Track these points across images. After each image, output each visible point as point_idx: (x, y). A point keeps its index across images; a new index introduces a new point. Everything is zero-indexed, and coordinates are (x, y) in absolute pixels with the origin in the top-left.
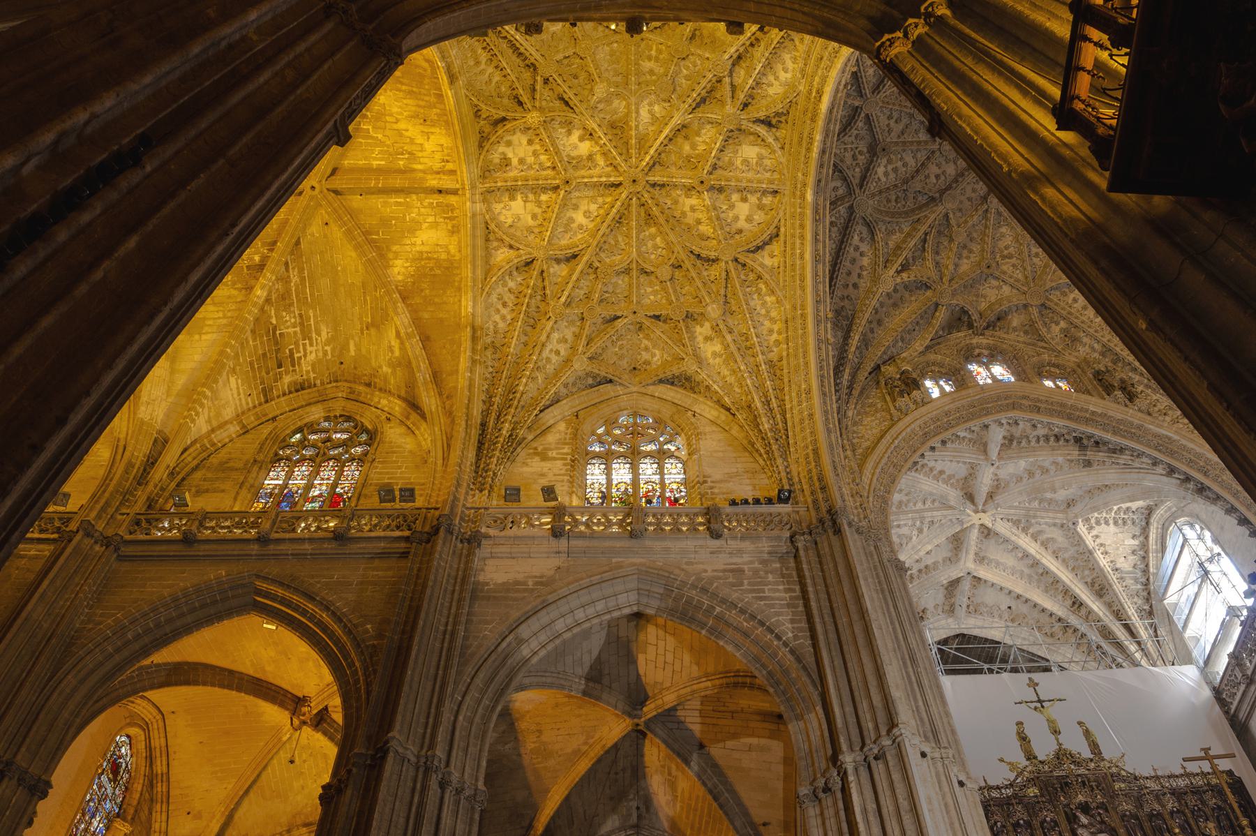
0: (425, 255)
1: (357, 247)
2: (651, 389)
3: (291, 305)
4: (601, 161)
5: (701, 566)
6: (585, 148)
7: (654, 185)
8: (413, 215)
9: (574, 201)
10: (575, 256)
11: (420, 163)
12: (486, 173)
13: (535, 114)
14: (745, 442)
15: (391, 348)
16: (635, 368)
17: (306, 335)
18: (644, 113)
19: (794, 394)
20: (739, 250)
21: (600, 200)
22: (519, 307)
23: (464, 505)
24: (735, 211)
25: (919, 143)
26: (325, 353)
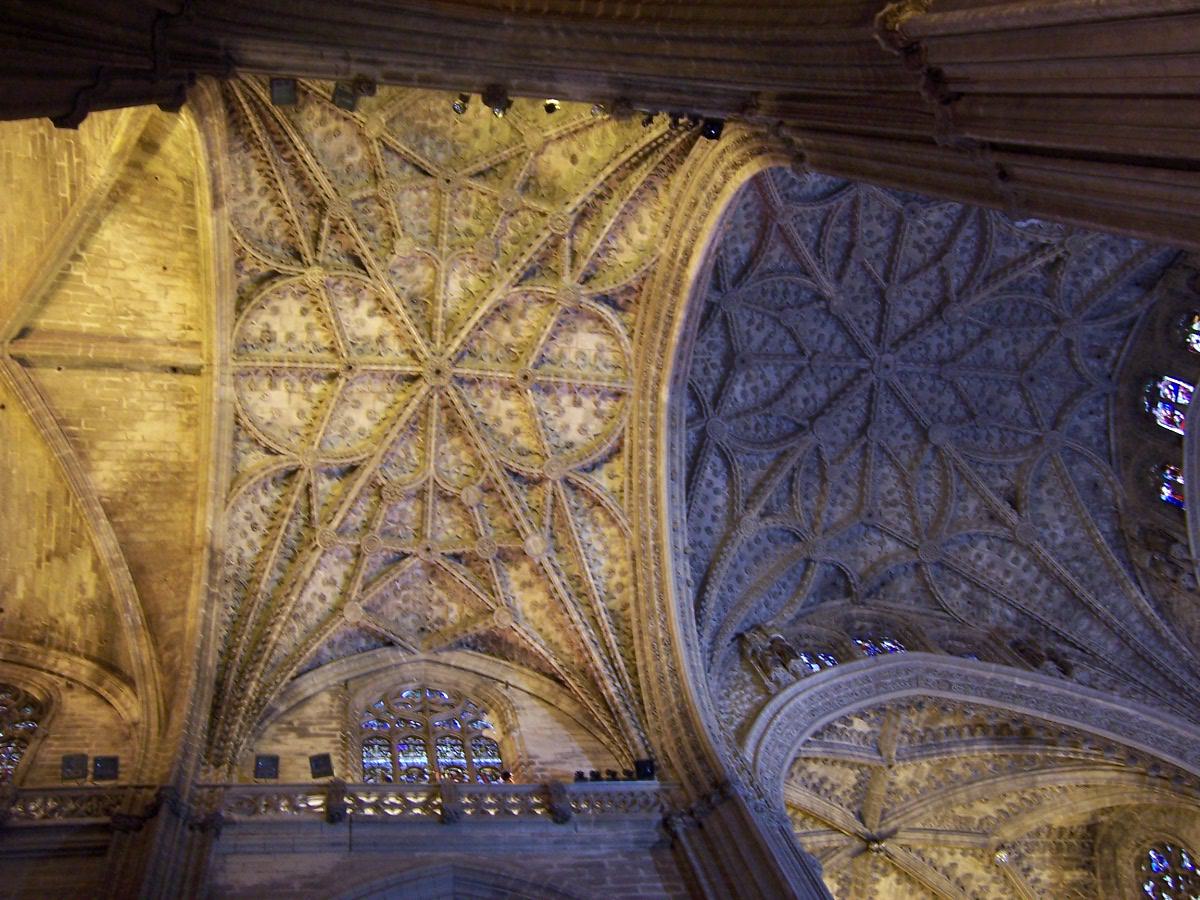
0: (146, 456)
1: (45, 440)
2: (445, 656)
4: (394, 345)
5: (542, 861)
6: (375, 326)
7: (461, 381)
8: (134, 401)
9: (356, 396)
10: (353, 469)
11: (151, 330)
12: (242, 347)
13: (317, 270)
14: (579, 717)
15: (82, 589)
16: (423, 629)
18: (455, 288)
19: (647, 648)
20: (571, 467)
21: (390, 397)
22: (274, 530)
23: (193, 783)
25: (785, 356)
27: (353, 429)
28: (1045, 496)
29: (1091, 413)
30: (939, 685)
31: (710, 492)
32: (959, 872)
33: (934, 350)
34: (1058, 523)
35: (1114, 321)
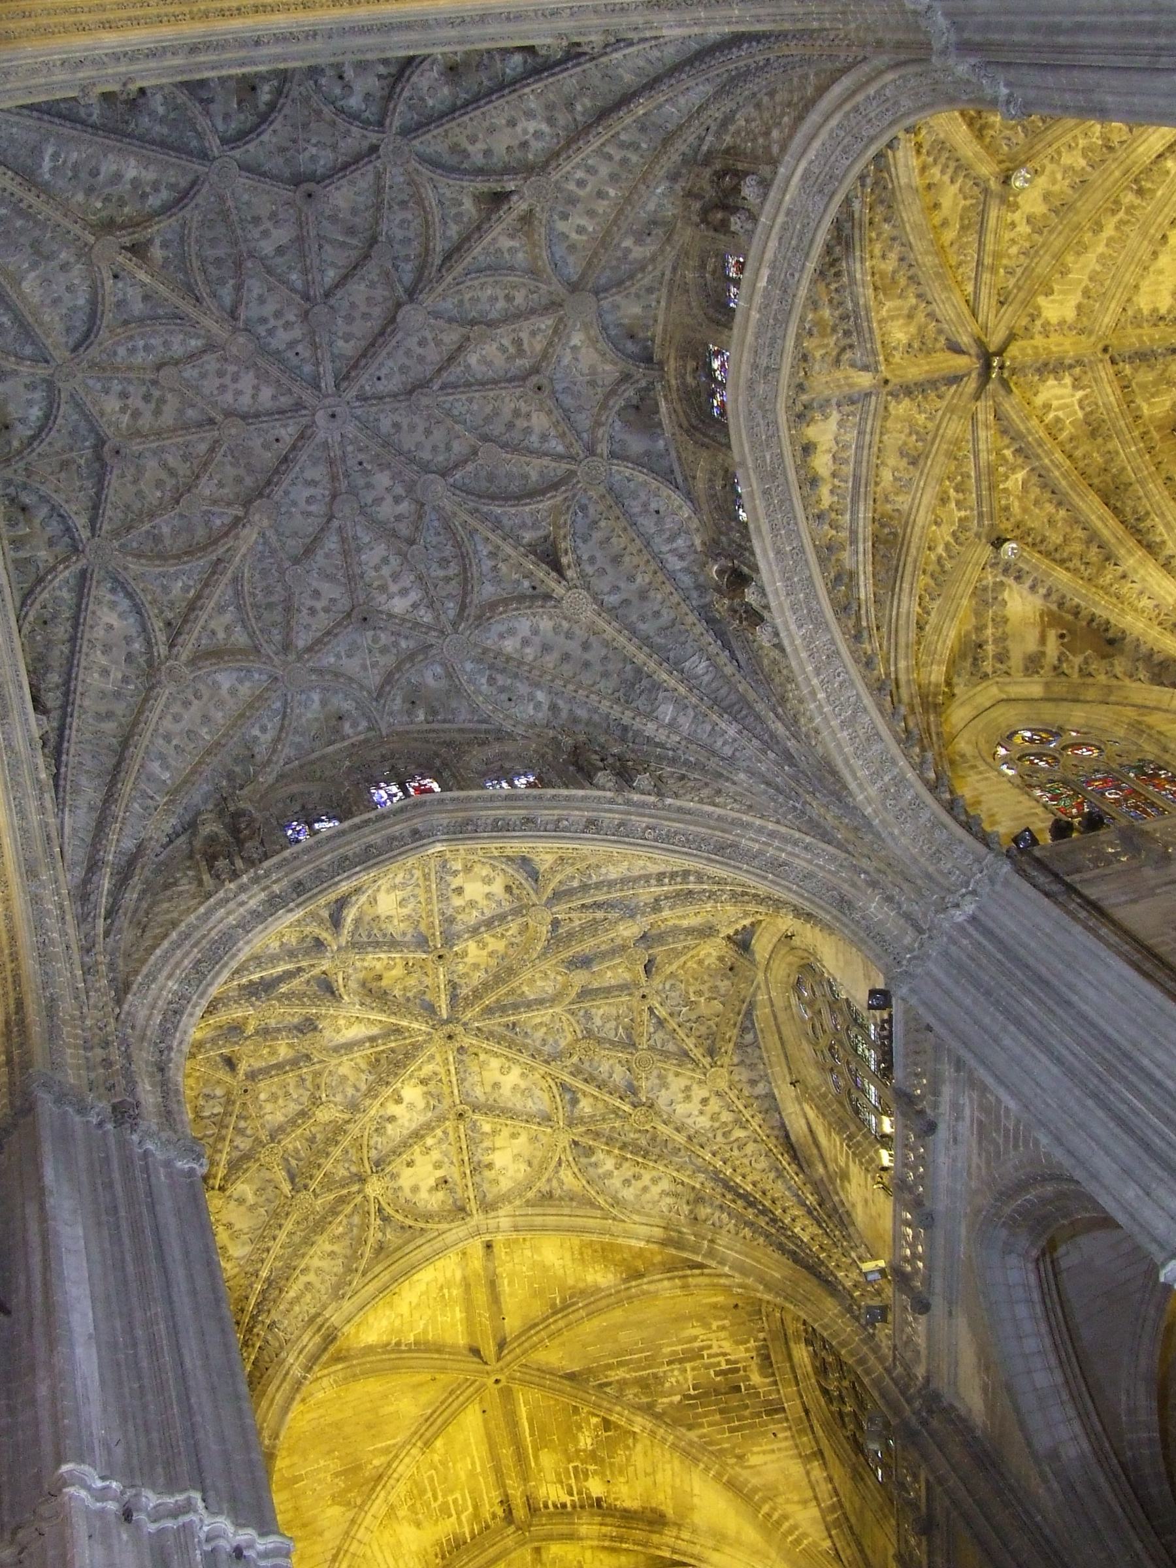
3: (655, 1376)
7: (454, 997)
9: (488, 1089)
12: (460, 1211)
17: (696, 1355)
26: (723, 1328)
27: (523, 1084)
28: (480, 146)
29: (341, 77)
31: (536, 640)
32: (1040, 209)
33: (297, 333)
34: (519, 129)
35: (196, 109)
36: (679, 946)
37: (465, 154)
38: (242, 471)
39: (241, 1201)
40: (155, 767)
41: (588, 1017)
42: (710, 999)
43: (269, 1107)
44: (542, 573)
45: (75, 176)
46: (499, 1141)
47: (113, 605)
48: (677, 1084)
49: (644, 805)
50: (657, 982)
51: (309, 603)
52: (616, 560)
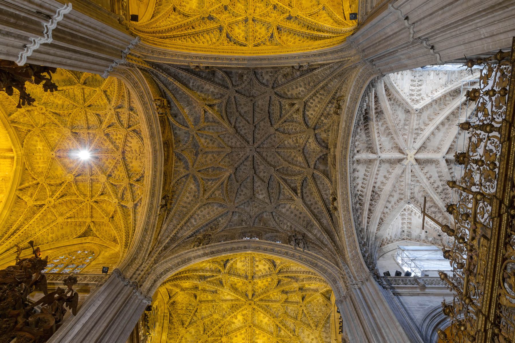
4: (244, 312)
6: (240, 317)
7: (253, 295)
13: (222, 339)
18: (229, 297)
24: (262, 269)
30: (346, 151)
33: (246, 131)
35: (227, 79)
36: (310, 293)
37: (287, 95)
38: (230, 160)
39: (191, 333)
40: (193, 221)
41: (287, 308)
42: (319, 312)
43: (204, 311)
44: (293, 194)
45: (198, 88)
46: (260, 337)
47: (193, 184)
48: (307, 333)
49: (300, 251)
50: (305, 302)
51: (240, 192)
52: (311, 194)
